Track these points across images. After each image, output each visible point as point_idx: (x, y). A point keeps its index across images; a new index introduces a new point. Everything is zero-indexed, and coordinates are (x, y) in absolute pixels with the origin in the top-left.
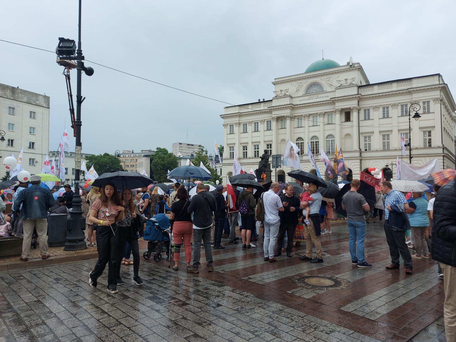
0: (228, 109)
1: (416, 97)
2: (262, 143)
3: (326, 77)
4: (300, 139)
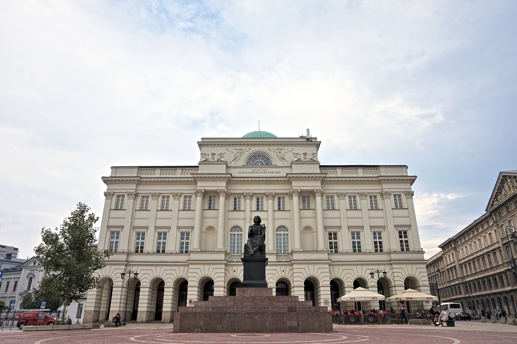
0: (118, 169)
1: (386, 187)
3: (275, 148)
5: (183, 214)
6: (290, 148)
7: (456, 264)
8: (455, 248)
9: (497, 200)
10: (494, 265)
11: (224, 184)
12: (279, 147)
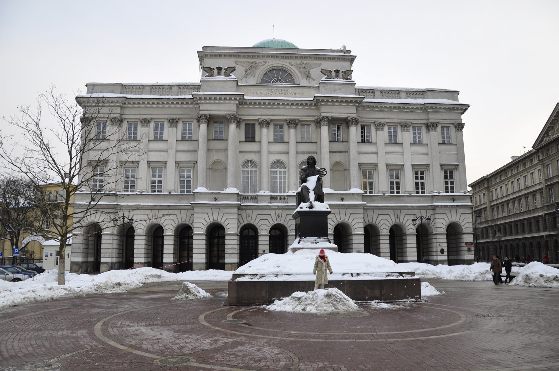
2: (171, 166)
3: (299, 62)
4: (250, 163)
5: (184, 146)
6: (318, 62)
7: (487, 205)
8: (488, 188)
9: (548, 136)
10: (532, 209)
11: (234, 108)
12: (303, 61)
